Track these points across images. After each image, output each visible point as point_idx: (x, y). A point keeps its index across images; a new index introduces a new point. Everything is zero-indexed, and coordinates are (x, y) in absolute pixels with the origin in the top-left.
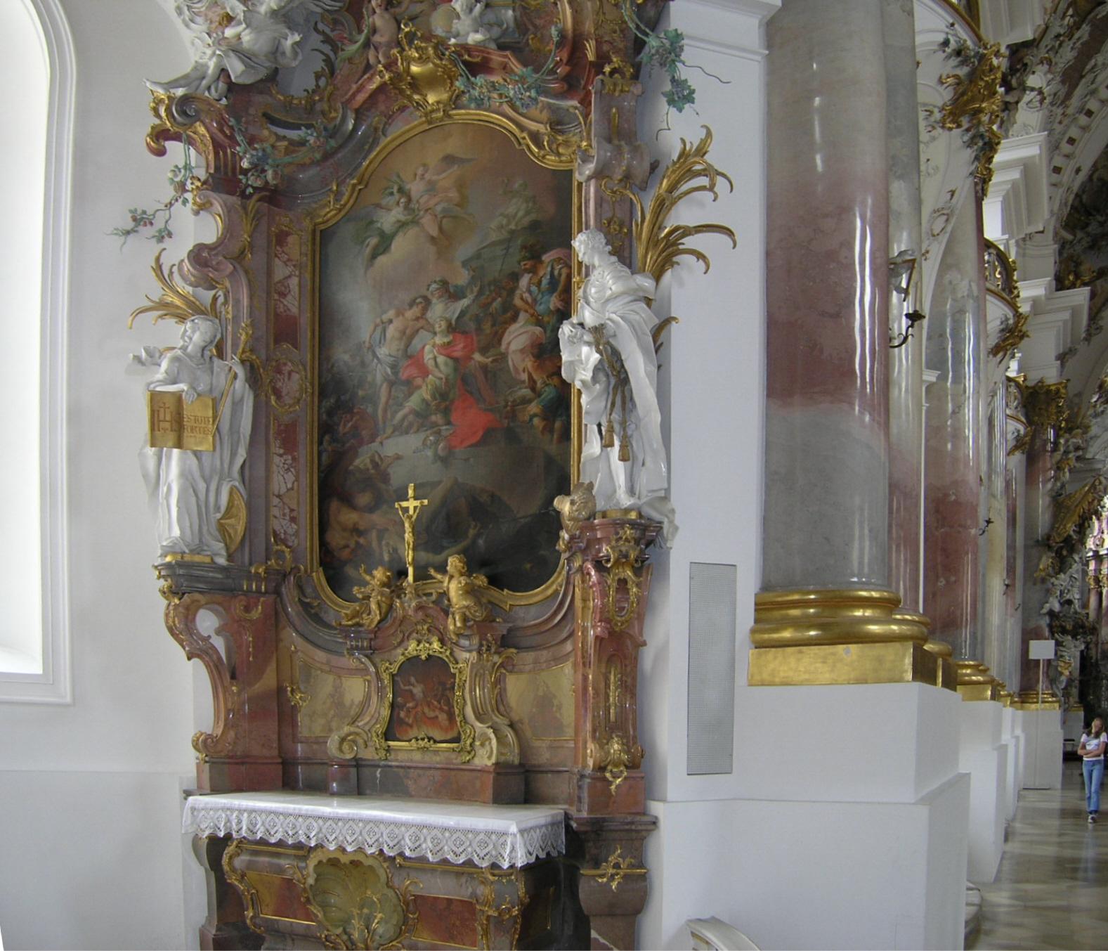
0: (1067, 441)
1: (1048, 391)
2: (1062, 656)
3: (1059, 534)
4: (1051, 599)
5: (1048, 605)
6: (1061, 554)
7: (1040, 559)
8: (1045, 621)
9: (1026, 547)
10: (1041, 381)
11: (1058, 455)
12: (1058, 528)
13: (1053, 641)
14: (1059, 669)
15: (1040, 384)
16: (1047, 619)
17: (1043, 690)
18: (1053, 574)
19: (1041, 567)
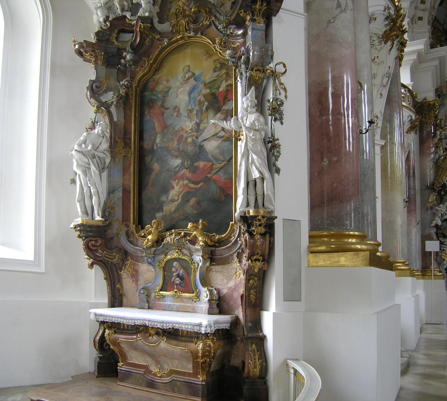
0: (441, 133)
1: (429, 105)
2: (444, 250)
3: (439, 183)
4: (436, 218)
5: (435, 222)
6: (441, 194)
7: (429, 196)
8: (433, 231)
9: (421, 190)
10: (425, 99)
11: (436, 140)
12: (438, 179)
13: (439, 241)
14: (443, 257)
15: (424, 101)
16: (435, 230)
17: (434, 269)
18: (437, 205)
19: (430, 201)
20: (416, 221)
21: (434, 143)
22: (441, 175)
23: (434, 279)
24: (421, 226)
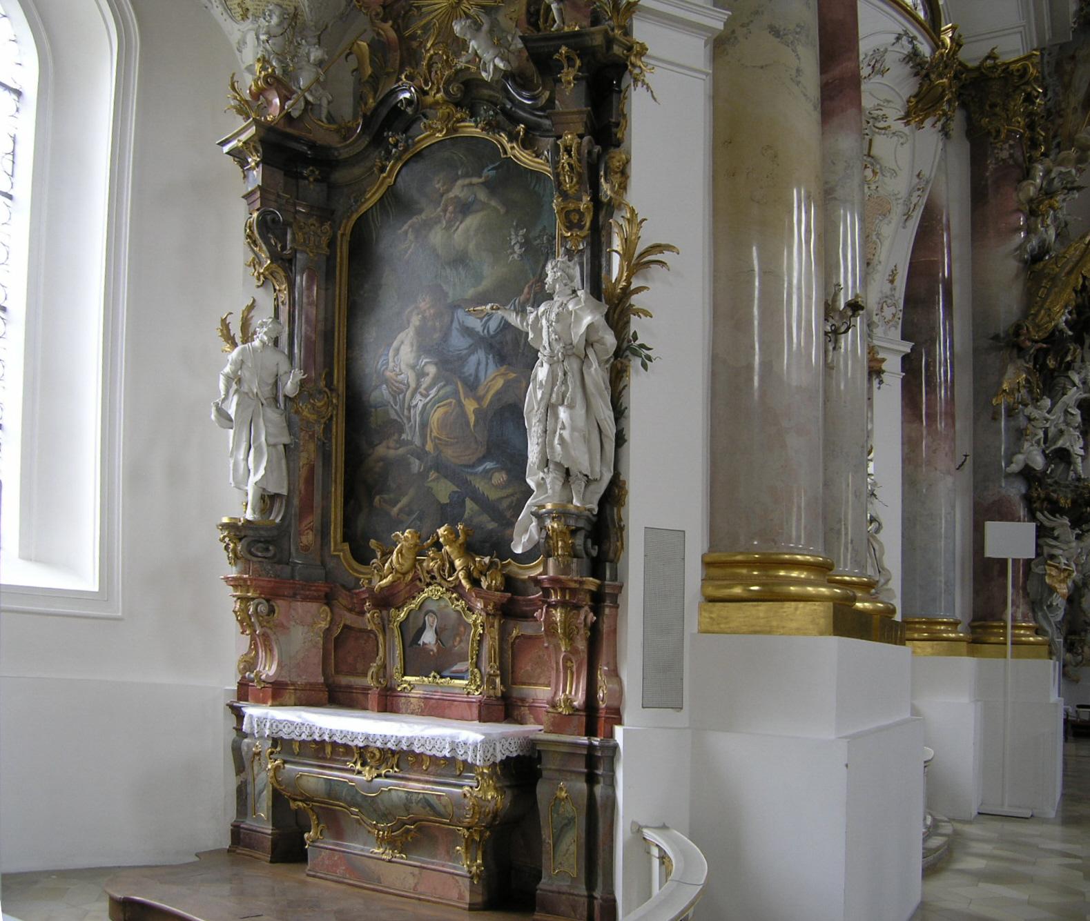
0: (1047, 172)
2: (1052, 557)
3: (1038, 327)
4: (1026, 445)
6: (1044, 365)
7: (1002, 372)
8: (1016, 490)
11: (1031, 189)
12: (1036, 315)
13: (1033, 525)
15: (989, 62)
17: (1014, 619)
18: (1029, 401)
19: (1005, 386)
20: (953, 452)
21: (1022, 196)
22: (1044, 300)
23: (1012, 657)
24: (975, 472)
